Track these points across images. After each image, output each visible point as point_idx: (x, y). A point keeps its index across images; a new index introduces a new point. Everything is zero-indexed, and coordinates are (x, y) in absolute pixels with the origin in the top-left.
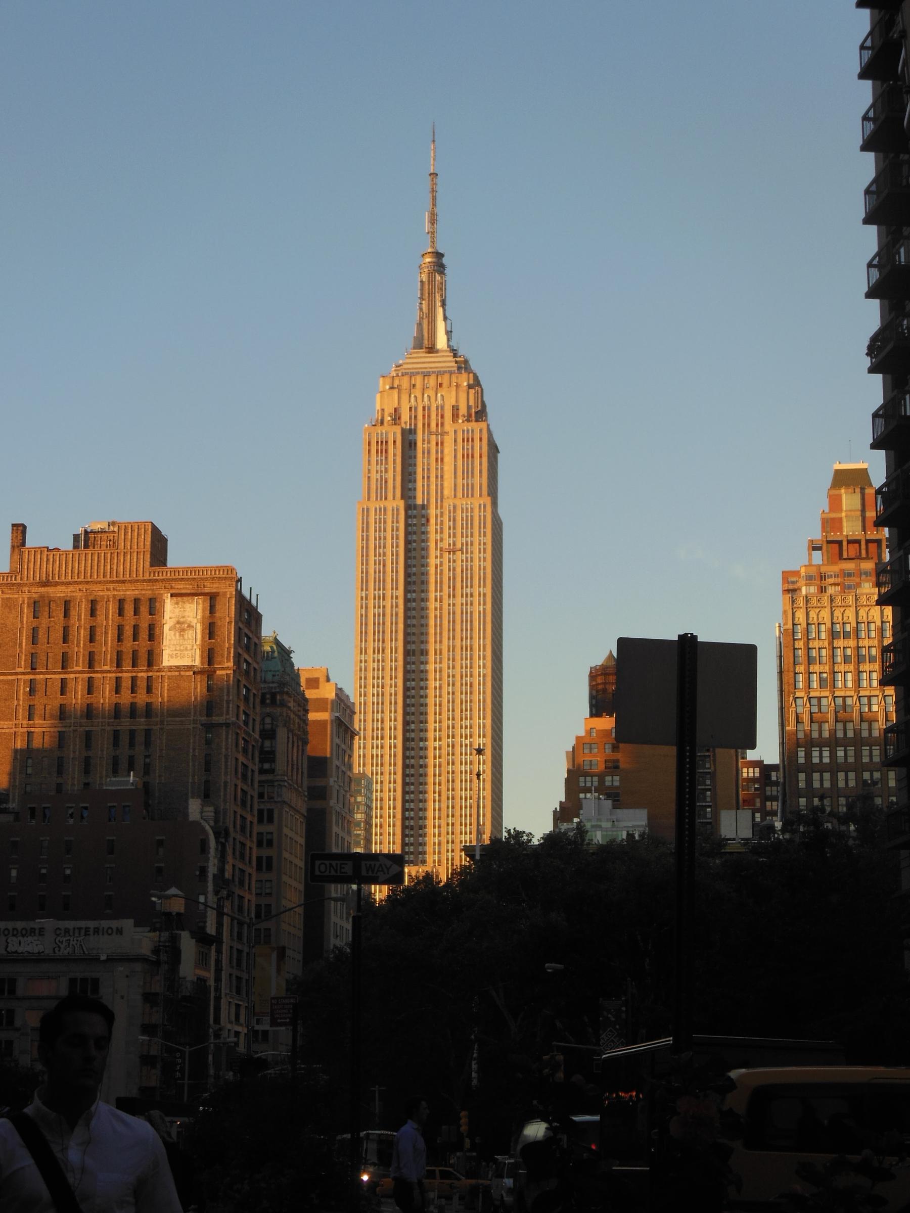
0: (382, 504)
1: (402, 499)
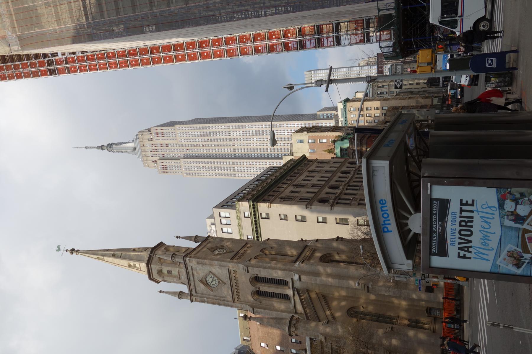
1: (179, 160)
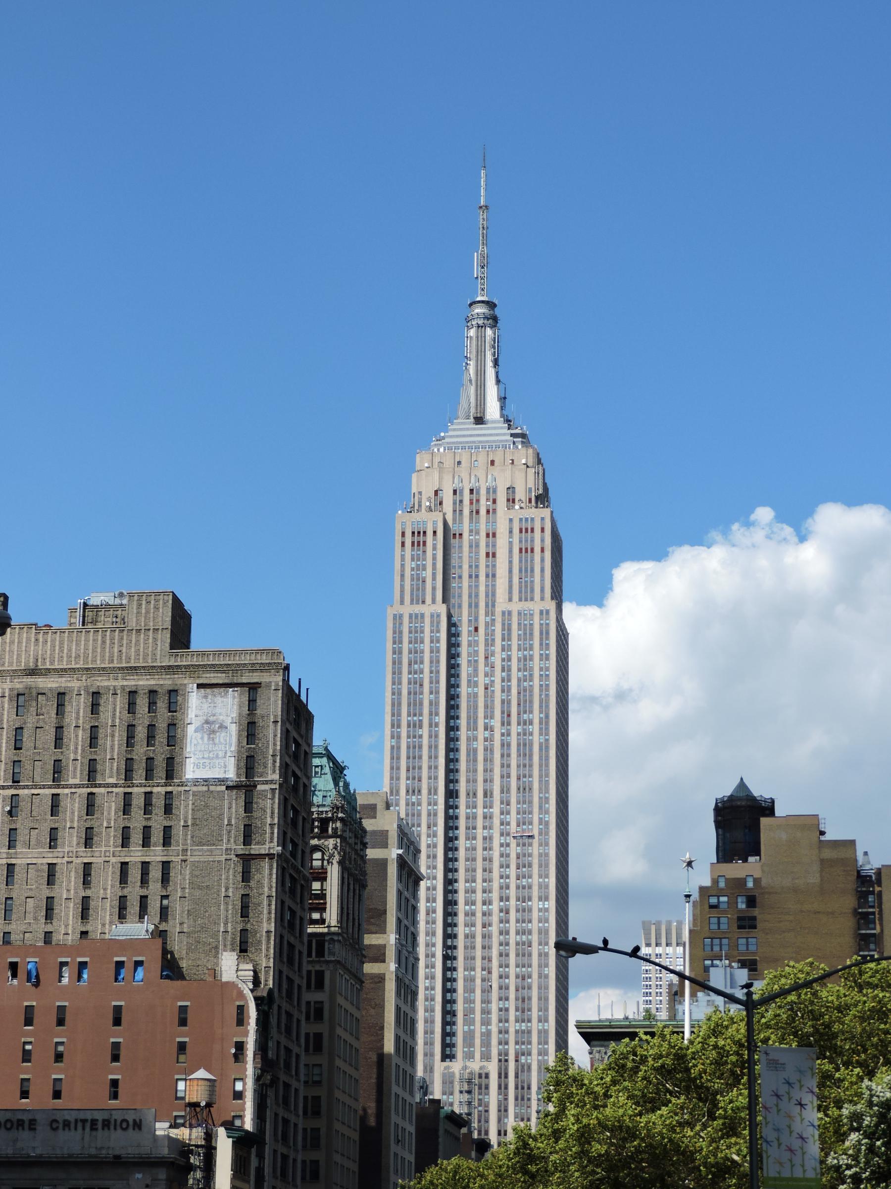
0: (418, 609)
